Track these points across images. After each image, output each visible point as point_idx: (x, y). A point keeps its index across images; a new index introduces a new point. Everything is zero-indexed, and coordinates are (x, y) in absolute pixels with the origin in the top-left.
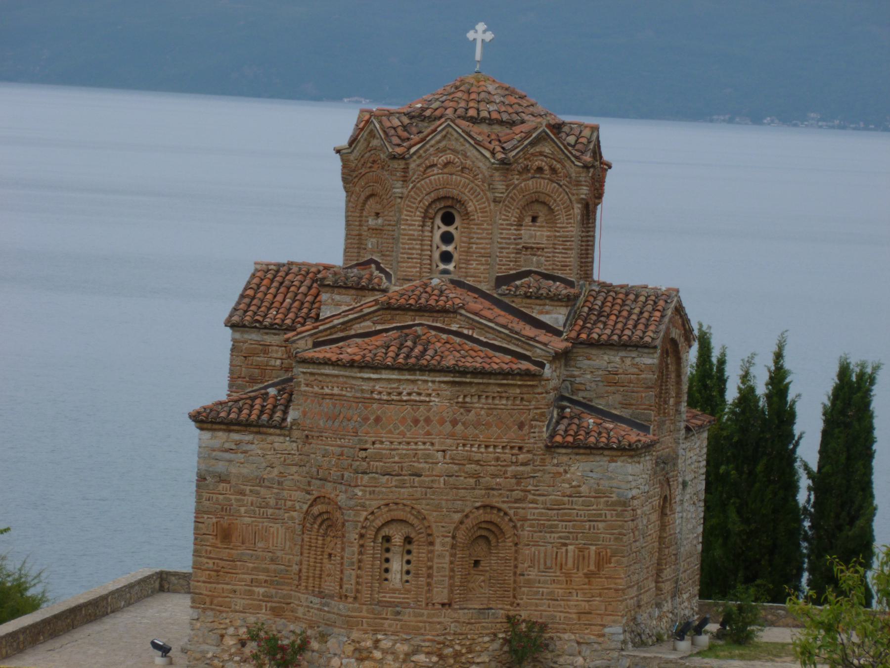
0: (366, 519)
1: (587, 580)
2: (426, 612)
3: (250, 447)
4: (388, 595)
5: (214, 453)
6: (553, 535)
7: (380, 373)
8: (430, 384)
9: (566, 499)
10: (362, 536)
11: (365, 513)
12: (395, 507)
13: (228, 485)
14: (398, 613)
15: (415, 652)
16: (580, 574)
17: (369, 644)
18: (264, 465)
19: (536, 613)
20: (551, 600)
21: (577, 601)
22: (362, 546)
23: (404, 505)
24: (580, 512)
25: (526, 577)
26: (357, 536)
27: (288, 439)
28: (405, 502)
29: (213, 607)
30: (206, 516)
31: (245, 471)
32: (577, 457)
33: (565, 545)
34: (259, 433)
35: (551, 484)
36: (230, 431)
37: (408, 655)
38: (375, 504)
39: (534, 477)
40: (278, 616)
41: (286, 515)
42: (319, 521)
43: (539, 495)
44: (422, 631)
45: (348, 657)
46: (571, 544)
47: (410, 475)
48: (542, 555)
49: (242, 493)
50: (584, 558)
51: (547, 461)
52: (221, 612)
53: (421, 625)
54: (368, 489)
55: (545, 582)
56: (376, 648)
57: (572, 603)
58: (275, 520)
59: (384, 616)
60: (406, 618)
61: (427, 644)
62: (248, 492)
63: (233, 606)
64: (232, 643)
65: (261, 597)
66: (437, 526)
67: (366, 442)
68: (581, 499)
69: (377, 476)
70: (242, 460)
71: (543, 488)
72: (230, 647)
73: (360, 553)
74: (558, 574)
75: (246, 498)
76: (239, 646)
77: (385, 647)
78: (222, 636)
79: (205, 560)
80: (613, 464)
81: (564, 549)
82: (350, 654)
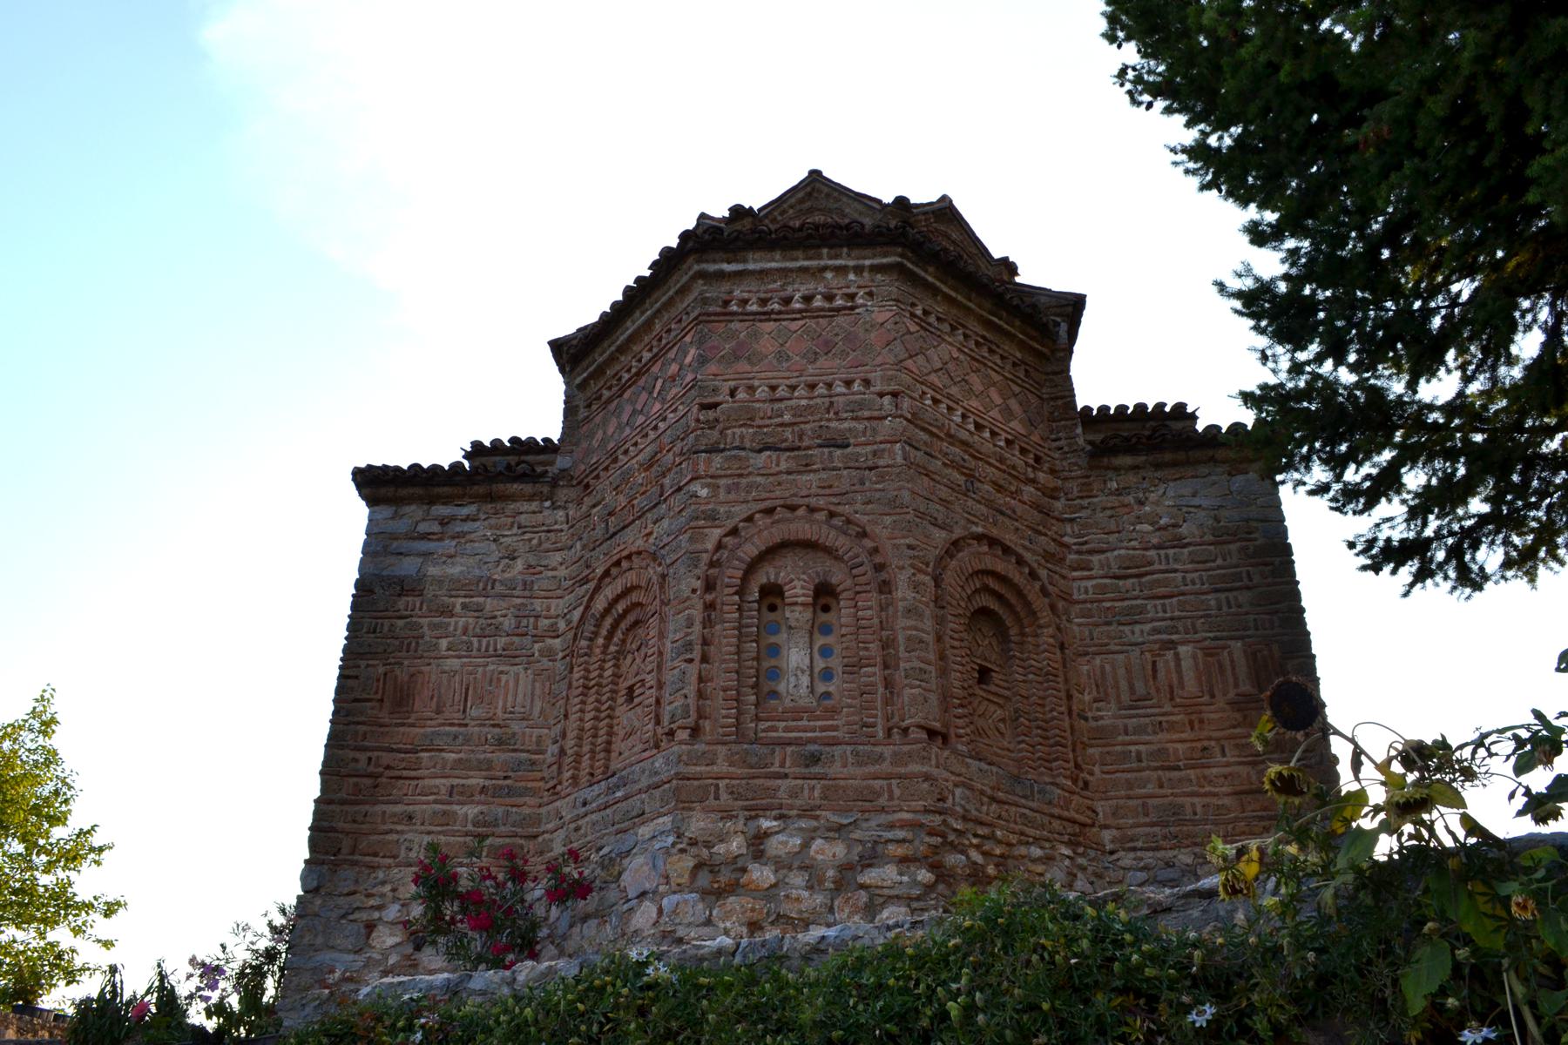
0: (720, 546)
1: (1238, 716)
2: (887, 751)
4: (783, 724)
6: (1137, 628)
7: (745, 261)
8: (852, 277)
9: (1152, 553)
10: (710, 586)
11: (717, 532)
12: (789, 515)
13: (418, 601)
14: (815, 759)
15: (870, 859)
16: (1220, 702)
17: (736, 845)
18: (496, 556)
19: (1130, 802)
20: (1163, 768)
21: (1228, 765)
22: (710, 607)
23: (812, 510)
24: (1189, 576)
25: (1093, 724)
26: (698, 584)
27: (547, 504)
28: (813, 501)
29: (356, 857)
32: (1158, 474)
33: (1172, 645)
34: (490, 498)
35: (1113, 527)
36: (432, 501)
37: (846, 868)
38: (741, 511)
39: (1072, 520)
41: (537, 646)
43: (1090, 552)
44: (883, 801)
45: (680, 889)
46: (1183, 643)
47: (820, 446)
48: (1121, 672)
50: (1221, 666)
51: (1096, 486)
52: (373, 868)
53: (877, 784)
54: (722, 482)
55: (1141, 730)
56: (758, 855)
57: (1214, 771)
58: (509, 656)
59: (775, 768)
60: (836, 769)
61: (900, 834)
62: (458, 608)
63: (403, 853)
64: (391, 941)
65: (470, 827)
66: (896, 546)
67: (715, 390)
68: (1186, 551)
69: (743, 453)
70: (452, 551)
71: (1095, 538)
72: (385, 954)
73: (707, 623)
74: (1168, 708)
75: (452, 620)
76: (409, 949)
77: (782, 851)
78: (370, 927)
79: (352, 754)
80: (1240, 478)
81: (1170, 655)
82: (685, 880)
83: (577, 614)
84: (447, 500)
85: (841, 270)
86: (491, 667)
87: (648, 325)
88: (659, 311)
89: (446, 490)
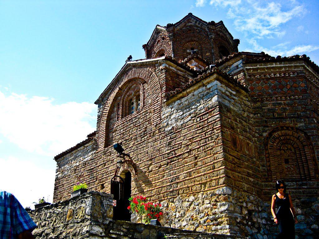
3: (234, 97)
5: (223, 95)
7: (309, 68)
30: (225, 129)
31: (235, 109)
40: (259, 197)
42: (278, 141)
49: (236, 121)
62: (238, 121)
83: (265, 134)
84: (230, 87)
86: (248, 141)
87: (281, 68)
88: (286, 67)
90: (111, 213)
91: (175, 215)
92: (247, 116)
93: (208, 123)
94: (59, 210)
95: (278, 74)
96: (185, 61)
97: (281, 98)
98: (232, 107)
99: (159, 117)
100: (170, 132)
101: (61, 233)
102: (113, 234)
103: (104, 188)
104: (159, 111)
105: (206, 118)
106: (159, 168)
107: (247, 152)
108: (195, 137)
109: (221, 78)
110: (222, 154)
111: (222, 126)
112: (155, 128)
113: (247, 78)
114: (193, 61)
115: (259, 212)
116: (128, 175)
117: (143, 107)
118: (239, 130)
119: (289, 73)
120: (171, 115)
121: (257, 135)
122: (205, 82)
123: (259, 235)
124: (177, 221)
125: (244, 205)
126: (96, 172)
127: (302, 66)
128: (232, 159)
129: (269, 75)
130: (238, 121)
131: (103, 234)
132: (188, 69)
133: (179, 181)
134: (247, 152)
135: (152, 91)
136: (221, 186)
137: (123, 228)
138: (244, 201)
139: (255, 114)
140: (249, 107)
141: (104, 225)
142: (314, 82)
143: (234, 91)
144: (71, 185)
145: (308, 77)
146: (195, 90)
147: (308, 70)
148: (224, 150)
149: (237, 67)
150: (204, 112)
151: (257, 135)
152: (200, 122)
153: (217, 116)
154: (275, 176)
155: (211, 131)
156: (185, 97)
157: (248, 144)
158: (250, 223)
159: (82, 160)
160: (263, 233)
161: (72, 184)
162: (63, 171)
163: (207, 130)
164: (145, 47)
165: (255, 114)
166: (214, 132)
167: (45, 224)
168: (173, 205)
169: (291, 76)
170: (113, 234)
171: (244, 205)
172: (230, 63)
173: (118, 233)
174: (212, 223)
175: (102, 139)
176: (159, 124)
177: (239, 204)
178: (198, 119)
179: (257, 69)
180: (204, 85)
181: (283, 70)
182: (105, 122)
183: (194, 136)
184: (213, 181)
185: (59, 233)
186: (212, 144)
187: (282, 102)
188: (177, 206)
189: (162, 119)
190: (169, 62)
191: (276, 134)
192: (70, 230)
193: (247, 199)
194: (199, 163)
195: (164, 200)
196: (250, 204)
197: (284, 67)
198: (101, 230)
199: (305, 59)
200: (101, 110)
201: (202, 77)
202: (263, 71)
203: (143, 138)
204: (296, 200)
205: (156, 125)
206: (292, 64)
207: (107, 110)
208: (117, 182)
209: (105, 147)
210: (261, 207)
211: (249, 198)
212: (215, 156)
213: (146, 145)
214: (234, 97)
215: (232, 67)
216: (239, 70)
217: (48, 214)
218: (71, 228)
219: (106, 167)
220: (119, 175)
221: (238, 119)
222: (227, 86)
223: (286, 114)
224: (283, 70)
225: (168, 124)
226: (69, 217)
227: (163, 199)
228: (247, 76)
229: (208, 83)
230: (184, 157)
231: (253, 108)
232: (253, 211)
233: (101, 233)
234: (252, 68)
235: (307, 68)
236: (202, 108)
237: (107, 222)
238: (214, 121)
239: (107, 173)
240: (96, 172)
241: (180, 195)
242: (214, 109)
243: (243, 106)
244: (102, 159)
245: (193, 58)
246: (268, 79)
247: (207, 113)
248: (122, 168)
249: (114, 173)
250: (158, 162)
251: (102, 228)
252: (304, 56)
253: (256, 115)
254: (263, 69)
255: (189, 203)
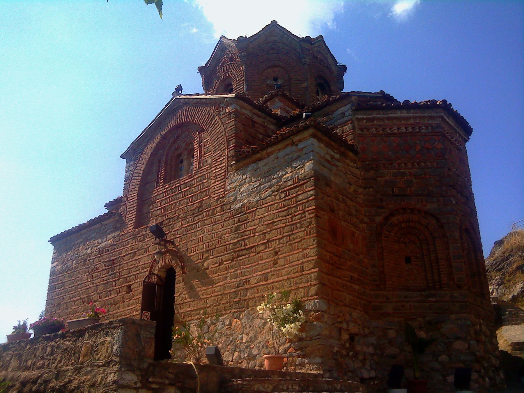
3: (337, 163)
7: (449, 119)
30: (322, 212)
31: (337, 181)
49: (338, 200)
62: (341, 199)
83: (378, 219)
85: (460, 135)
86: (352, 229)
87: (408, 118)
88: (416, 117)
89: (333, 143)
90: (151, 351)
91: (242, 339)
92: (355, 191)
93: (297, 202)
94: (68, 343)
95: (403, 128)
96: (264, 99)
97: (405, 164)
98: (332, 178)
99: (223, 187)
100: (239, 211)
101: (70, 382)
102: (153, 383)
103: (131, 291)
104: (223, 177)
105: (295, 195)
106: (220, 265)
107: (351, 246)
108: (275, 222)
109: (319, 134)
110: (316, 249)
111: (318, 208)
112: (215, 203)
113: (357, 132)
114: (277, 100)
115: (365, 336)
116: (170, 273)
117: (199, 169)
118: (341, 213)
119: (419, 127)
120: (241, 185)
121: (366, 219)
122: (296, 139)
123: (363, 370)
124: (244, 347)
125: (345, 326)
126: (120, 265)
127: (439, 117)
128: (330, 256)
129: (390, 129)
130: (341, 199)
131: (139, 385)
132: (269, 114)
133: (248, 286)
134: (351, 246)
135: (213, 148)
136: (311, 298)
137: (169, 372)
138: (345, 319)
139: (365, 188)
140: (357, 178)
141: (140, 370)
142: (455, 140)
143: (337, 153)
144: (77, 283)
145: (447, 133)
146: (279, 150)
147: (448, 122)
148: (319, 245)
149: (343, 114)
150: (291, 185)
151: (366, 219)
152: (285, 200)
153: (311, 192)
154: (390, 282)
155: (300, 215)
156: (264, 159)
157: (353, 234)
158: (351, 353)
159: (96, 244)
160: (369, 368)
161: (79, 283)
162: (64, 261)
163: (295, 212)
164: (201, 70)
165: (365, 188)
166: (305, 217)
167: (43, 364)
168: (239, 322)
169: (423, 131)
170: (153, 383)
171: (345, 326)
172: (333, 108)
173: (160, 381)
174: (296, 354)
175: (131, 215)
176: (222, 197)
177: (337, 325)
178: (283, 195)
179: (373, 120)
180: (293, 144)
181: (411, 121)
182: (137, 188)
183: (275, 220)
184: (301, 290)
185: (66, 380)
186: (300, 234)
187: (407, 171)
188: (244, 324)
189: (227, 191)
190: (241, 102)
191: (394, 220)
192: (85, 377)
193: (348, 317)
194: (281, 262)
195: (225, 314)
196: (353, 324)
197: (413, 117)
198: (135, 378)
199: (446, 106)
200: (131, 169)
201: (292, 131)
202: (381, 123)
203: (196, 218)
204: (419, 319)
205: (218, 199)
206: (424, 113)
207: (140, 170)
208: (153, 283)
209: (135, 228)
210: (369, 328)
211: (351, 315)
212: (305, 252)
213: (200, 228)
214: (337, 163)
215: (336, 114)
216: (345, 119)
217: (49, 349)
218: (87, 373)
219: (135, 258)
220: (156, 272)
221: (341, 196)
222: (328, 145)
223: (411, 190)
224: (411, 121)
225: (236, 199)
226: (84, 357)
227: (224, 312)
228: (357, 129)
229: (300, 141)
230: (259, 250)
231: (363, 179)
232: (357, 335)
233: (136, 383)
234: (365, 117)
235: (447, 120)
236: (289, 178)
237: (145, 366)
238: (306, 200)
239: (138, 269)
240: (120, 265)
241: (250, 308)
242: (308, 181)
243: (349, 176)
244: (130, 245)
245: (276, 95)
246: (388, 135)
247: (296, 187)
248: (161, 261)
249: (149, 269)
250: (218, 255)
251: (137, 375)
252: (444, 101)
253: (367, 190)
254: (382, 119)
255: (263, 321)
